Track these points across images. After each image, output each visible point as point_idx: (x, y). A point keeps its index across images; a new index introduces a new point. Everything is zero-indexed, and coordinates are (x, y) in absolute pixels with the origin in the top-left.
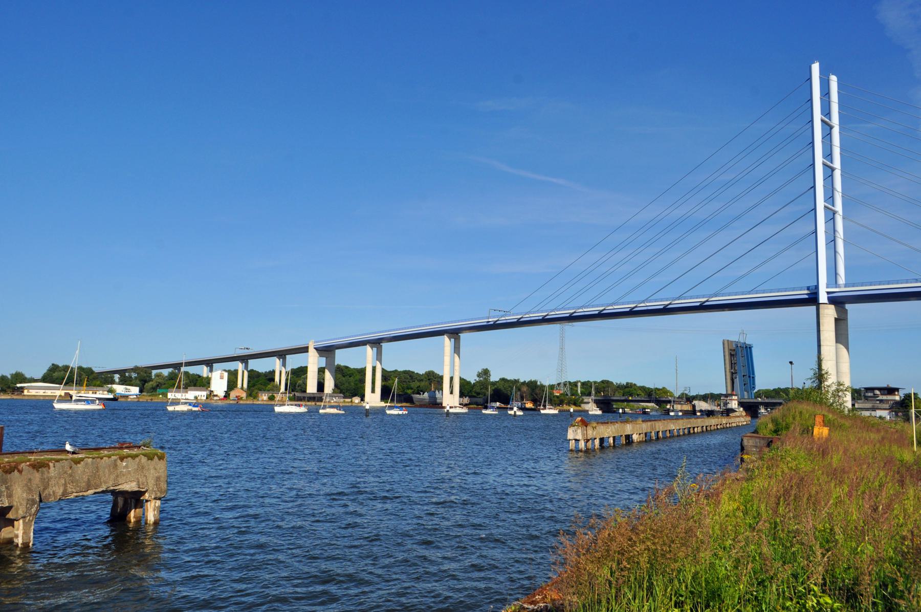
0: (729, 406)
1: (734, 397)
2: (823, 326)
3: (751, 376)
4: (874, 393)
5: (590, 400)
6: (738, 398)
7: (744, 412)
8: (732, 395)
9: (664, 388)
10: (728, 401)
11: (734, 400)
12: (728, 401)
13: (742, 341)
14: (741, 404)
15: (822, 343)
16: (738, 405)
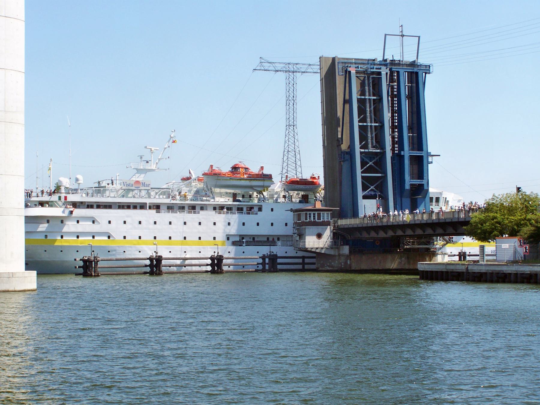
13: (409, 58)
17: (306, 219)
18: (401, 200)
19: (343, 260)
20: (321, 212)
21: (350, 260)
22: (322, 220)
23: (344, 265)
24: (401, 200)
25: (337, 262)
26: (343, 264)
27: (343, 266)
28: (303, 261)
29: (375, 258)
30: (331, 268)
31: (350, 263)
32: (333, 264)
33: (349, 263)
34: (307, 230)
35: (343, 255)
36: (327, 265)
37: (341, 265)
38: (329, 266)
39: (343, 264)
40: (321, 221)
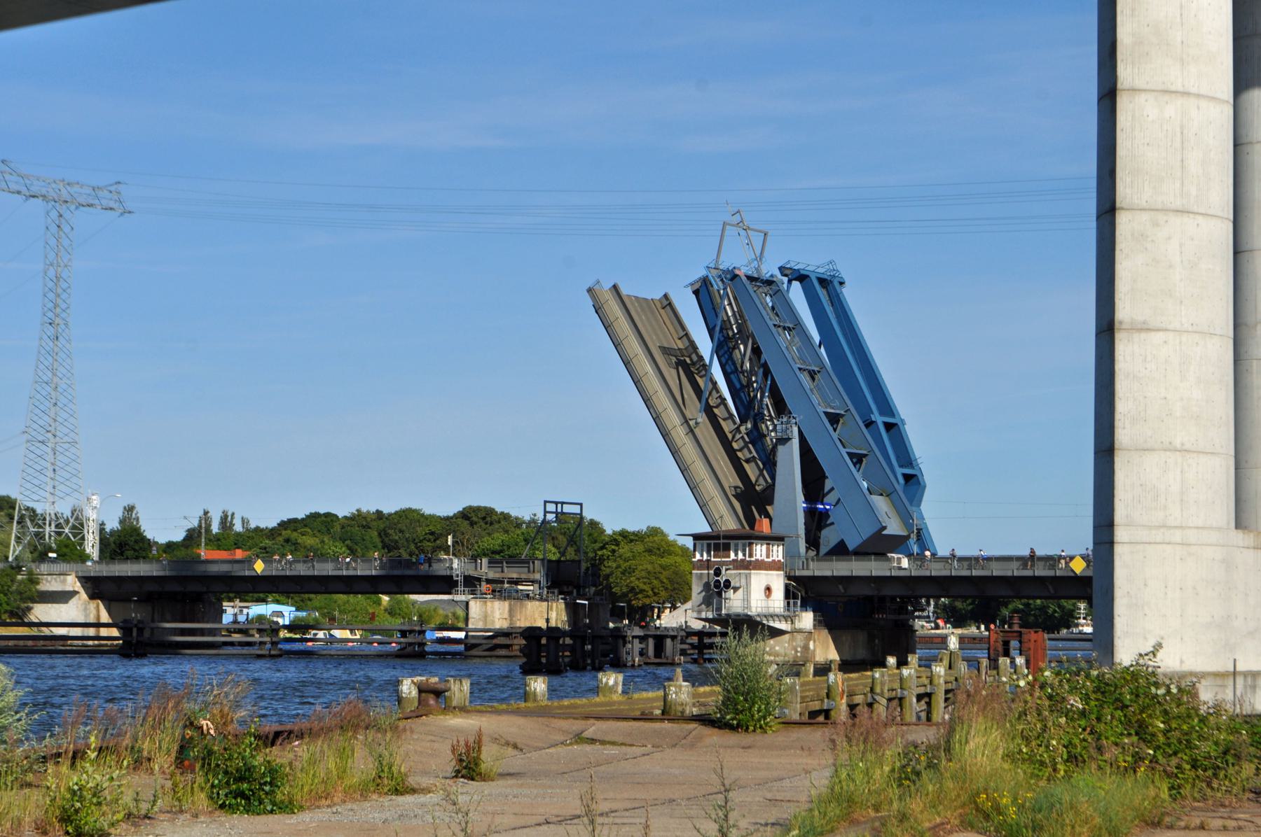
0: (734, 603)
1: (760, 551)
3: (879, 419)
5: (71, 582)
6: (786, 554)
7: (825, 634)
8: (748, 537)
9: (655, 532)
10: (726, 574)
11: (760, 565)
12: (726, 574)
16: (789, 594)
17: (751, 556)
21: (814, 642)
22: (770, 560)
23: (801, 652)
26: (799, 649)
27: (799, 654)
28: (701, 640)
29: (844, 638)
31: (814, 646)
32: (777, 648)
34: (752, 576)
35: (800, 631)
37: (796, 651)
39: (799, 649)
40: (731, 559)
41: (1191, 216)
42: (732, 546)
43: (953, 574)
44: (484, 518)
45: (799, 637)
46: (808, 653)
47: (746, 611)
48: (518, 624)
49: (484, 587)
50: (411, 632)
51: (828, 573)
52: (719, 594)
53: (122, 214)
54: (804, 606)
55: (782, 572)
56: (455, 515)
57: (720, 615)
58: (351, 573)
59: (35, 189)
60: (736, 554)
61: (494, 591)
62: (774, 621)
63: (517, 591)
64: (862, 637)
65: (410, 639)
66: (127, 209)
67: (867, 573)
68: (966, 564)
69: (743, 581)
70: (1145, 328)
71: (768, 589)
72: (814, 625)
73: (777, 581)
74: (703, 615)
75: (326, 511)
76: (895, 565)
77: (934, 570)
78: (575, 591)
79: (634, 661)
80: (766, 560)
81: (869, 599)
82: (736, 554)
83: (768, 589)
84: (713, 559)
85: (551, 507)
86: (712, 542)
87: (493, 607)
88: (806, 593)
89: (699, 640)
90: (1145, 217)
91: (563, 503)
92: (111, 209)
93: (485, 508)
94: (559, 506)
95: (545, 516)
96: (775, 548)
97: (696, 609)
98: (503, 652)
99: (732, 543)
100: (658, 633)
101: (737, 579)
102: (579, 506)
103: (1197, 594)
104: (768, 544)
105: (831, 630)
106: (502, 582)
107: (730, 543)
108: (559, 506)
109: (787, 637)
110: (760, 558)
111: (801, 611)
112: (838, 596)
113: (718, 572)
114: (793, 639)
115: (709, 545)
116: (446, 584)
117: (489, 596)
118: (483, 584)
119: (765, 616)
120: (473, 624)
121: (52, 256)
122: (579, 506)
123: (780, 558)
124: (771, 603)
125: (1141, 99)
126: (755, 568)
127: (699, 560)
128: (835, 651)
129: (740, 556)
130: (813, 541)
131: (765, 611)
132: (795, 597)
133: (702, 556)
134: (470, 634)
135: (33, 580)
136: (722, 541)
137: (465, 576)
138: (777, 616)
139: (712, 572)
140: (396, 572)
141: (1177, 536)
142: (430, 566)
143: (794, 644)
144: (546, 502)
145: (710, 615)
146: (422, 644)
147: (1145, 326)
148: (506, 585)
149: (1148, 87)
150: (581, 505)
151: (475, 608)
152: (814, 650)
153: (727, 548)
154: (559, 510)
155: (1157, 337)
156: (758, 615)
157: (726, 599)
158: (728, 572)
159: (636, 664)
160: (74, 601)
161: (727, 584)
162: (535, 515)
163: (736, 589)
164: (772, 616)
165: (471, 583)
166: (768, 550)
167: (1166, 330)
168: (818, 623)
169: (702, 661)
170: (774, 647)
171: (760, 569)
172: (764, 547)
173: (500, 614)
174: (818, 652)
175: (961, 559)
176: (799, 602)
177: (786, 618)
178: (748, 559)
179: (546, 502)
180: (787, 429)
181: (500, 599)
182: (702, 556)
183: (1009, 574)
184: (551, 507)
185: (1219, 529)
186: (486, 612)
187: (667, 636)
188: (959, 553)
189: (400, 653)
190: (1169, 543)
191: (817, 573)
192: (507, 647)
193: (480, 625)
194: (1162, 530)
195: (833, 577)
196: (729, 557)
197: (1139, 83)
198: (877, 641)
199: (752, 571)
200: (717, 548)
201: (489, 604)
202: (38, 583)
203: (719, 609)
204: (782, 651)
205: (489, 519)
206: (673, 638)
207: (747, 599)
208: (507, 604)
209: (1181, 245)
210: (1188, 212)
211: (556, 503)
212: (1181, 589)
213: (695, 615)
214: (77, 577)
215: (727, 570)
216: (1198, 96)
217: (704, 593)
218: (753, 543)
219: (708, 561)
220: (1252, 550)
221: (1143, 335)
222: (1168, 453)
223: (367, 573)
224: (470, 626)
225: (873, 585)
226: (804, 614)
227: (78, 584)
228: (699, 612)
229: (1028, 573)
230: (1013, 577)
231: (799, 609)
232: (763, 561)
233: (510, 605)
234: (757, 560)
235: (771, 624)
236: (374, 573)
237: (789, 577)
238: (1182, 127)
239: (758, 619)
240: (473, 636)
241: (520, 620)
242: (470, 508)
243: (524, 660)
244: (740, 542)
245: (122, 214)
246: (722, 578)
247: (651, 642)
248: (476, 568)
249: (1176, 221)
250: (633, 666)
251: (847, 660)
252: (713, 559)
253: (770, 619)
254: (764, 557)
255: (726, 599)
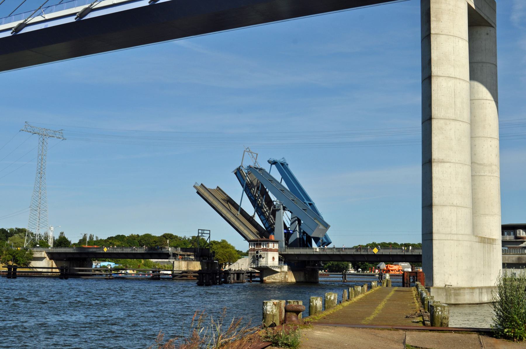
0: (262, 262)
1: (271, 246)
2: (438, 20)
4: (515, 234)
5: (44, 254)
6: (279, 247)
9: (224, 241)
10: (260, 253)
11: (271, 250)
12: (260, 253)
14: (284, 259)
15: (435, 70)
16: (280, 260)
17: (268, 247)
18: (430, 240)
19: (283, 275)
20: (264, 242)
22: (274, 248)
24: (430, 240)
25: (279, 276)
26: (283, 278)
27: (283, 279)
28: (251, 274)
29: (297, 274)
30: (275, 281)
32: (276, 277)
33: (287, 277)
35: (283, 272)
36: (272, 278)
37: (282, 278)
38: (273, 279)
39: (283, 278)
41: (458, 121)
42: (262, 244)
43: (334, 253)
44: (170, 237)
45: (283, 274)
46: (286, 279)
47: (266, 265)
48: (190, 269)
49: (179, 257)
50: (156, 271)
51: (293, 253)
52: (258, 260)
53: (63, 140)
54: (285, 263)
55: (278, 253)
56: (161, 236)
57: (258, 266)
58: (136, 252)
59: (35, 131)
60: (263, 247)
61: (182, 258)
62: (275, 268)
63: (190, 258)
64: (302, 274)
65: (155, 274)
66: (65, 138)
67: (306, 253)
68: (338, 250)
69: (266, 255)
70: (443, 162)
71: (273, 258)
72: (288, 270)
73: (276, 255)
74: (252, 266)
75: (122, 235)
76: (315, 250)
77: (328, 252)
78: (208, 259)
79: (231, 281)
80: (273, 248)
81: (304, 261)
82: (263, 247)
83: (273, 258)
84: (255, 248)
85: (200, 231)
86: (255, 242)
87: (182, 263)
88: (285, 259)
89: (250, 274)
90: (442, 121)
91: (204, 230)
92: (60, 138)
93: (170, 234)
94: (203, 231)
95: (198, 234)
96: (276, 244)
97: (250, 264)
98: (185, 278)
99: (262, 243)
100: (238, 272)
101: (264, 254)
102: (209, 231)
103: (462, 259)
104: (274, 243)
105: (293, 272)
106: (185, 255)
107: (261, 243)
108: (203, 231)
109: (279, 273)
110: (271, 248)
111: (284, 265)
112: (295, 260)
113: (257, 252)
114: (281, 274)
115: (254, 244)
116: (167, 256)
117: (181, 260)
118: (179, 256)
119: (273, 267)
120: (175, 269)
121: (40, 152)
122: (209, 231)
123: (277, 248)
124: (274, 263)
125: (440, 79)
126: (269, 251)
127: (251, 248)
128: (294, 279)
129: (265, 247)
130: (286, 244)
131: (272, 265)
132: (282, 261)
133: (252, 247)
134: (174, 272)
135: (31, 254)
136: (259, 242)
137: (173, 253)
138: (276, 267)
139: (255, 252)
140: (150, 252)
141: (455, 237)
142: (161, 250)
143: (281, 276)
144: (199, 230)
145: (255, 266)
146: (159, 275)
147: (443, 161)
148: (186, 256)
149: (443, 75)
150: (210, 231)
151: (176, 263)
152: (288, 278)
153: (260, 244)
154: (203, 232)
155: (447, 165)
156: (271, 267)
157: (260, 261)
158: (261, 252)
159: (232, 282)
160: (45, 260)
161: (261, 256)
162: (185, 236)
163: (263, 258)
164: (274, 267)
165: (175, 255)
166: (273, 245)
167: (450, 162)
168: (289, 269)
169: (251, 281)
170: (275, 277)
171: (271, 251)
172: (272, 244)
173: (184, 266)
174: (289, 278)
175: (337, 249)
176: (283, 262)
177: (279, 267)
178: (267, 248)
179: (199, 230)
180: (279, 206)
181: (184, 260)
182: (252, 247)
183: (353, 253)
184: (200, 231)
185: (469, 235)
186: (180, 265)
187: (241, 273)
188: (336, 247)
189: (152, 278)
190: (452, 240)
191: (289, 253)
192: (186, 276)
193: (178, 269)
194: (450, 235)
195: (294, 254)
196: (261, 247)
197: (440, 74)
198: (307, 275)
199: (269, 252)
200: (257, 244)
201: (181, 262)
202: (33, 254)
203: (258, 264)
204: (278, 278)
205: (171, 237)
206: (243, 274)
207: (267, 261)
208: (186, 262)
209: (455, 132)
210: (457, 120)
211: (202, 230)
212: (457, 257)
213: (249, 266)
214: (46, 253)
215: (260, 252)
216: (460, 79)
217: (252, 259)
218: (269, 243)
219: (254, 249)
220: (478, 243)
221: (442, 164)
222: (452, 207)
223: (141, 252)
224: (174, 269)
225: (307, 257)
226: (285, 266)
227: (46, 255)
228: (251, 265)
229: (359, 253)
230: (354, 255)
231: (283, 264)
232: (272, 249)
233: (187, 263)
234: (270, 248)
235: (274, 269)
236: (143, 252)
237: (280, 254)
238: (454, 90)
239: (270, 268)
240: (175, 273)
241: (190, 268)
242: (166, 234)
243: (198, 281)
244: (265, 243)
245: (63, 140)
246: (259, 254)
247: (236, 275)
248: (176, 251)
249: (453, 123)
250: (231, 283)
251: (298, 281)
252: (255, 248)
253: (274, 268)
254: (272, 248)
255: (260, 261)
